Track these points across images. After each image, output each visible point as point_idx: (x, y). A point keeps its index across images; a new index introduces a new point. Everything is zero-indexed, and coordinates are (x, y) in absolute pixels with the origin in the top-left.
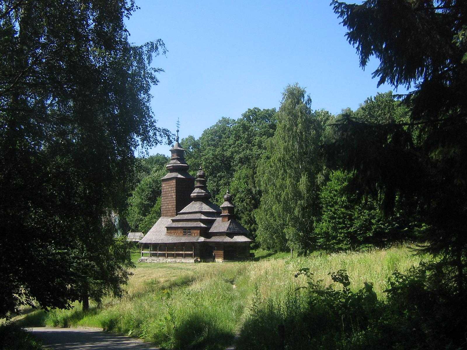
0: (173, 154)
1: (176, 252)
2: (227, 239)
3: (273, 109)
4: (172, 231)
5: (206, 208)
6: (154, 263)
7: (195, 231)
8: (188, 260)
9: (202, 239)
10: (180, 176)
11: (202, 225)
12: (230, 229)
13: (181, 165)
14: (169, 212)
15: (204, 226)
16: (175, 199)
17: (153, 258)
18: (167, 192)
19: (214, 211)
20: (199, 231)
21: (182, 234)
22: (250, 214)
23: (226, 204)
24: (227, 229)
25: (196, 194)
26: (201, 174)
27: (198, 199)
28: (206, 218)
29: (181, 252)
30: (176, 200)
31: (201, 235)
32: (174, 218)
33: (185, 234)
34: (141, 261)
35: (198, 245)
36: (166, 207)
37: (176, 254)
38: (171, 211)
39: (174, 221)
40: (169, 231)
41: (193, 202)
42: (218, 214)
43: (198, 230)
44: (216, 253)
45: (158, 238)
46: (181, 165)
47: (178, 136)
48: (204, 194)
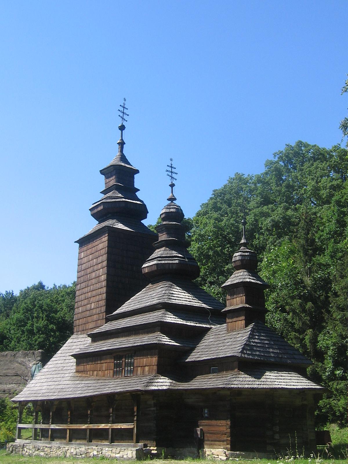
0: (108, 180)
1: (92, 426)
2: (244, 381)
3: (335, 147)
4: (88, 367)
5: (182, 297)
6: (38, 456)
7: (145, 360)
10: (120, 226)
11: (166, 340)
12: (252, 350)
13: (124, 200)
14: (90, 319)
15: (173, 343)
16: (104, 283)
17: (41, 444)
18: (89, 271)
19: (204, 305)
20: (154, 360)
21: (112, 371)
22: (304, 339)
23: (240, 276)
24: (243, 349)
25: (155, 262)
26: (172, 210)
27: (161, 274)
28: (180, 321)
29: (102, 426)
30: (108, 286)
31: (162, 371)
32: (96, 331)
33: (117, 372)
34: (12, 452)
35: (152, 402)
36: (84, 308)
37: (91, 430)
38: (95, 317)
40: (81, 368)
41: (150, 285)
42: (218, 315)
43: (152, 355)
44: (205, 429)
45: (52, 387)
46: (124, 200)
47: (122, 139)
48: (177, 262)
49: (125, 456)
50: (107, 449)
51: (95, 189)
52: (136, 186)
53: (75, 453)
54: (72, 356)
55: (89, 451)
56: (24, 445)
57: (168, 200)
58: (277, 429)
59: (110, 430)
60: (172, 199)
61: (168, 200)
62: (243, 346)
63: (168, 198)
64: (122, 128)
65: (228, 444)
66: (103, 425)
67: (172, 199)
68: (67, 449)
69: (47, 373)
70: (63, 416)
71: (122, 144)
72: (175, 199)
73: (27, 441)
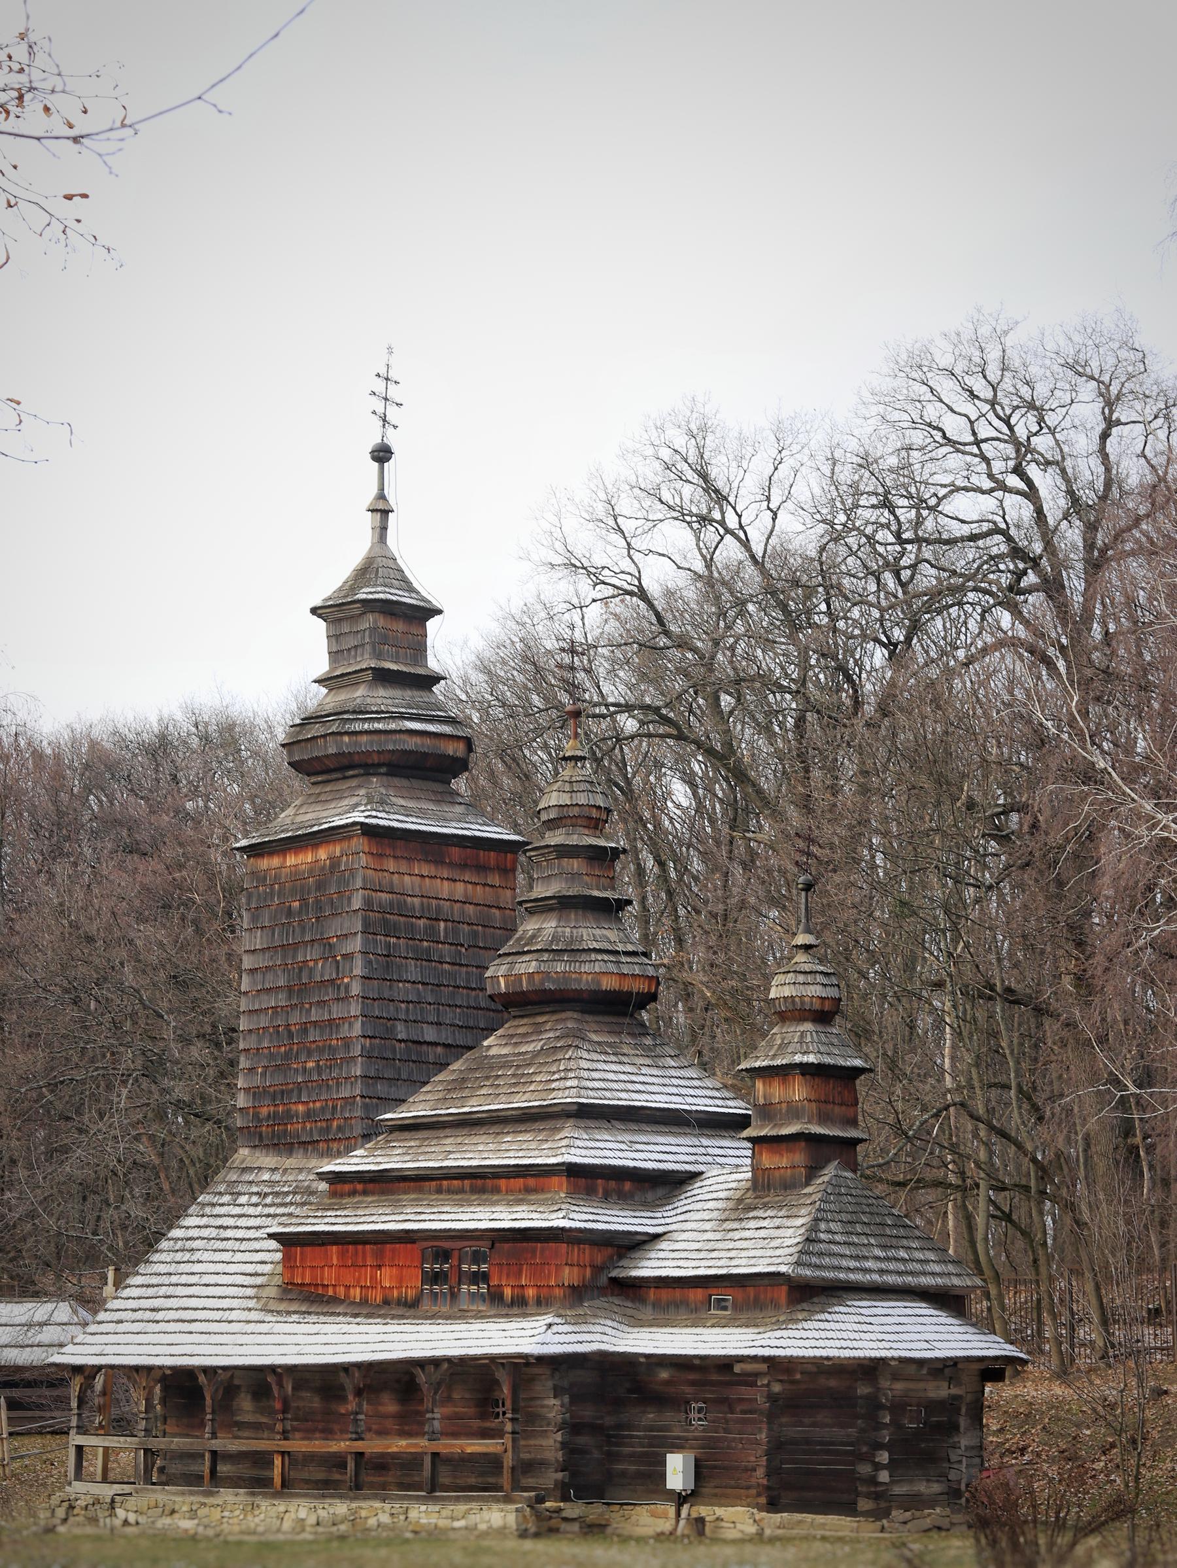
8: (462, 1508)
47: (381, 496)
54: (271, 1236)
55: (363, 1514)
56: (113, 1501)
59: (428, 1460)
62: (800, 1246)
64: (382, 454)
65: (759, 1495)
68: (282, 1509)
71: (382, 511)
73: (127, 1488)
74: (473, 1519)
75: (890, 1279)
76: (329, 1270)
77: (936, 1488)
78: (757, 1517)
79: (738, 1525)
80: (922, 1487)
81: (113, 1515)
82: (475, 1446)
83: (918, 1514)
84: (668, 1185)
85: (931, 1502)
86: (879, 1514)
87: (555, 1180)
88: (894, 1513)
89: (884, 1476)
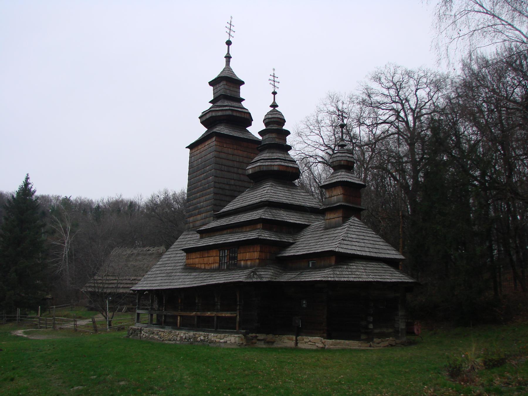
1: (199, 313)
9: (266, 275)
29: (209, 314)
31: (263, 263)
37: (199, 317)
39: (204, 233)
49: (228, 342)
50: (212, 334)
51: (204, 99)
52: (242, 96)
53: (184, 337)
54: (183, 250)
55: (197, 336)
57: (271, 106)
58: (371, 319)
60: (274, 106)
61: (271, 106)
63: (271, 104)
64: (229, 43)
66: (209, 313)
67: (274, 106)
69: (162, 266)
70: (172, 305)
71: (228, 57)
72: (277, 106)
74: (225, 339)
75: (373, 255)
76: (196, 259)
77: (390, 330)
78: (323, 341)
79: (317, 344)
80: (385, 330)
81: (141, 333)
82: (228, 314)
83: (383, 340)
84: (299, 228)
85: (388, 335)
86: (369, 340)
87: (259, 226)
88: (375, 340)
89: (371, 326)
